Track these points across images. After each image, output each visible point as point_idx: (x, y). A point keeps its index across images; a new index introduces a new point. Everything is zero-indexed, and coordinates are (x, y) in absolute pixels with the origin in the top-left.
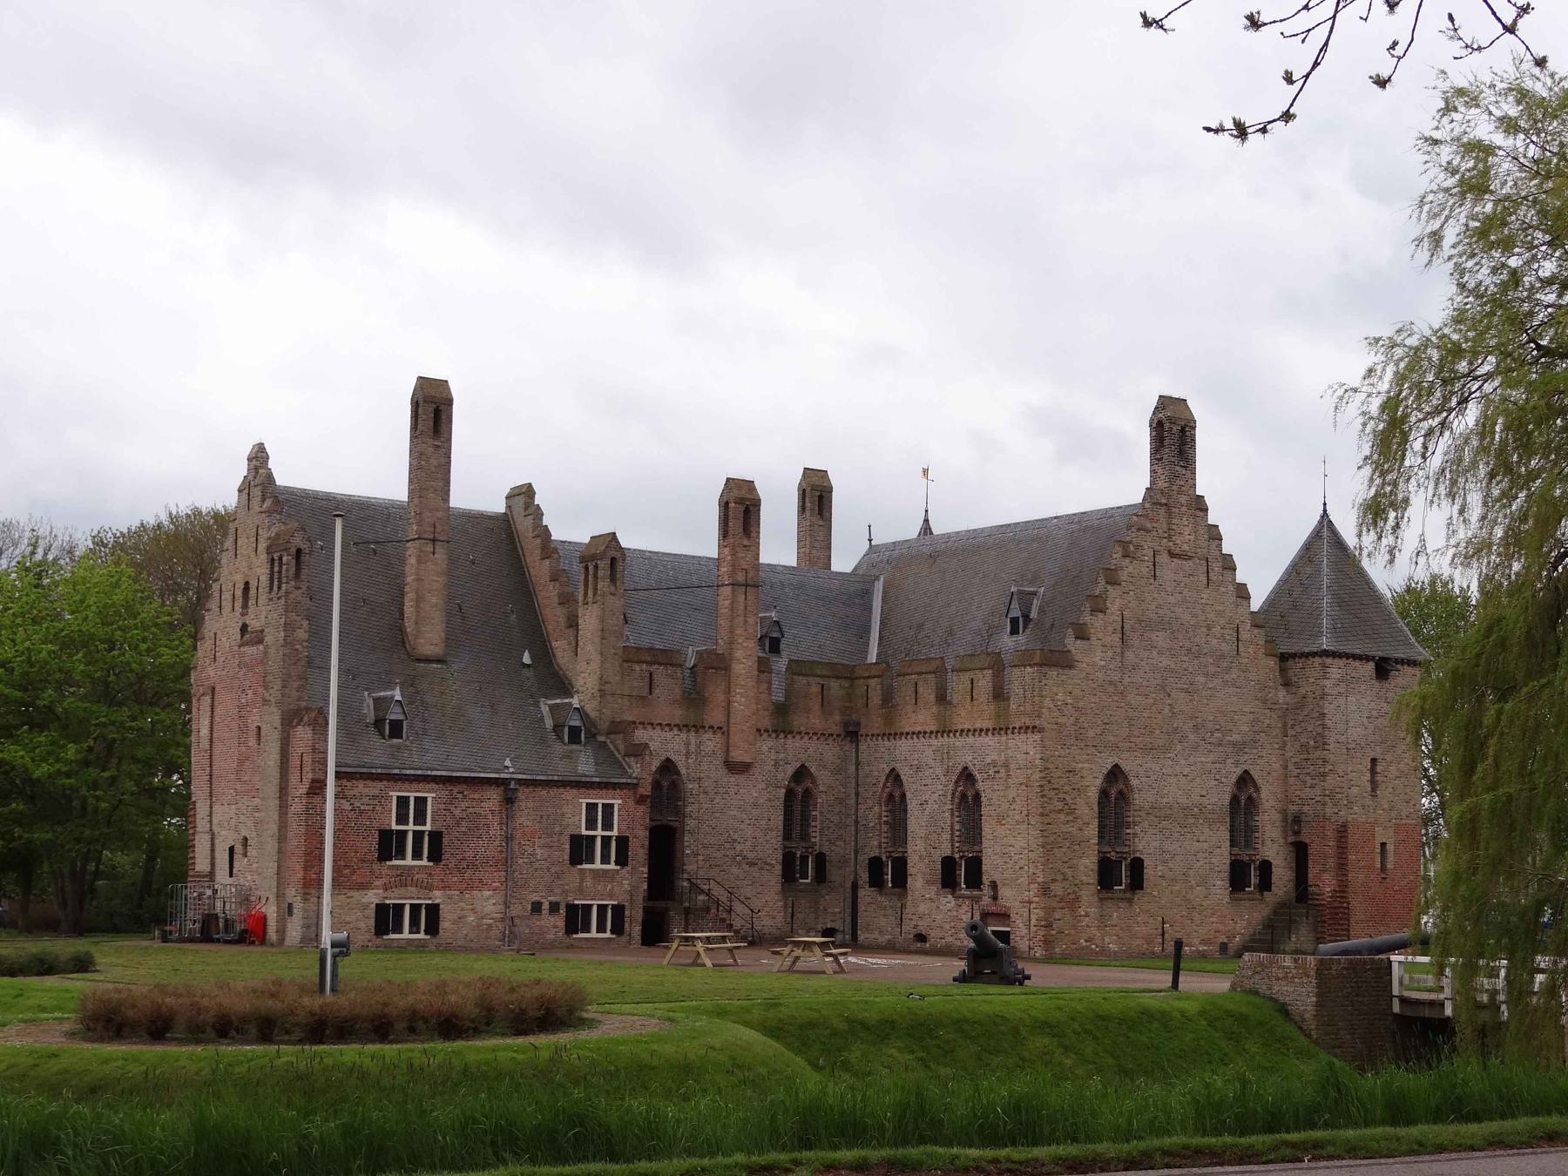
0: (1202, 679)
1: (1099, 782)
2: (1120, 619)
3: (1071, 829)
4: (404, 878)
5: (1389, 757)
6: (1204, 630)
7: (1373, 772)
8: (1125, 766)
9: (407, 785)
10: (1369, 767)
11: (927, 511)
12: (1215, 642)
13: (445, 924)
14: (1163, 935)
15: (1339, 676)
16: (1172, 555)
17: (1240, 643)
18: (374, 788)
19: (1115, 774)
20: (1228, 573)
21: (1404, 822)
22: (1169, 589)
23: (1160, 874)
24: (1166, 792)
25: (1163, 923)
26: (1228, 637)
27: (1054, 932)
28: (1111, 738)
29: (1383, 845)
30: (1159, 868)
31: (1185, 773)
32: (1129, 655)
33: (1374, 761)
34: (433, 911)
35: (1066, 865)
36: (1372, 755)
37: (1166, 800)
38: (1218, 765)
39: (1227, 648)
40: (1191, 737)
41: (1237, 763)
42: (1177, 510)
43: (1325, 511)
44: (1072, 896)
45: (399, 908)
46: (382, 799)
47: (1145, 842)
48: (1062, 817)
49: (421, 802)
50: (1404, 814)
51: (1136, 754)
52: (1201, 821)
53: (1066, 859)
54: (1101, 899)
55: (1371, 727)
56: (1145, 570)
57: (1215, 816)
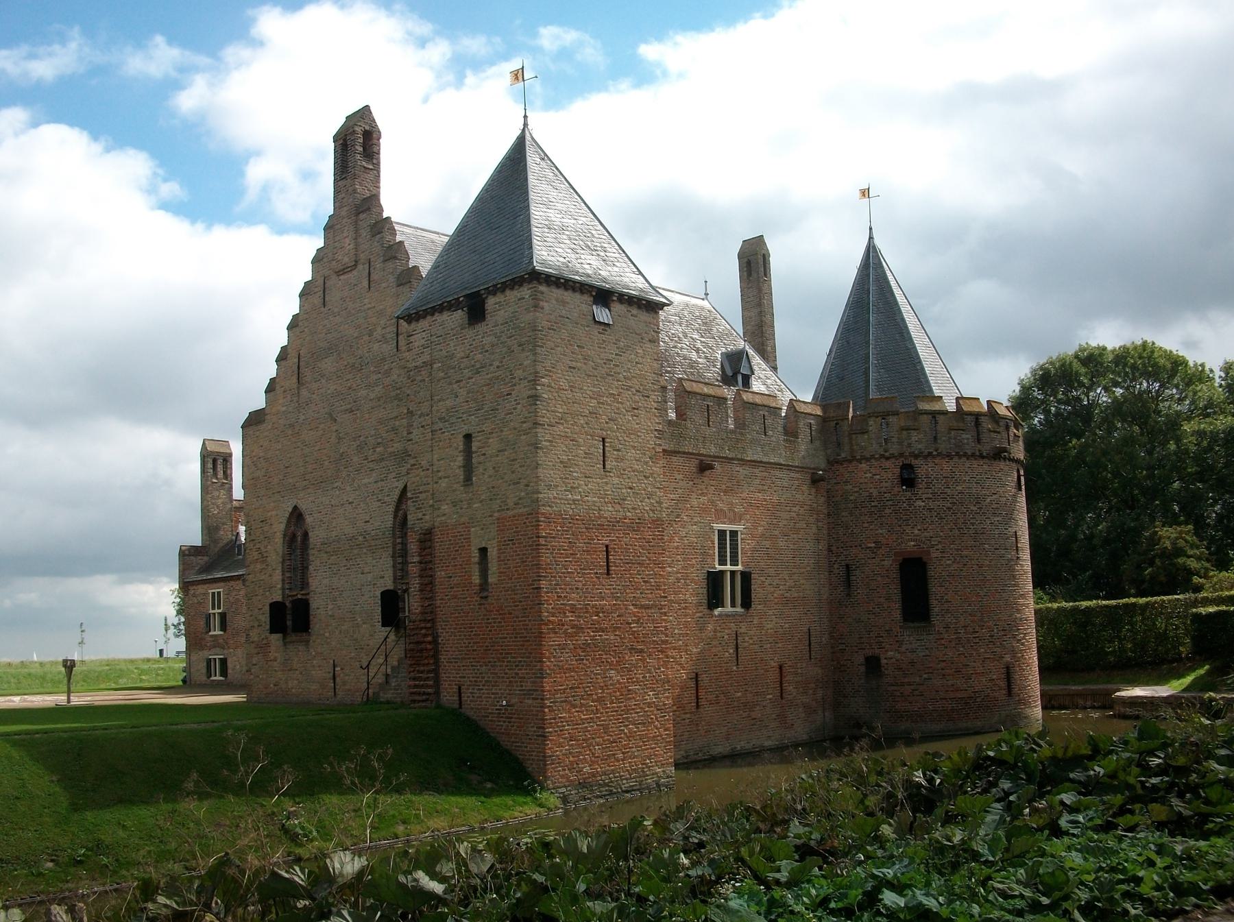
0: (363, 393)
1: (282, 526)
2: (296, 360)
3: (263, 577)
4: (216, 643)
5: (487, 427)
6: (366, 338)
7: (468, 452)
8: (303, 507)
9: (215, 585)
10: (461, 447)
11: (871, 229)
12: (376, 346)
13: (230, 671)
14: (334, 678)
15: (423, 342)
16: (339, 273)
17: (401, 337)
18: (206, 586)
19: (297, 516)
20: (390, 265)
21: (510, 513)
22: (336, 310)
23: (330, 613)
24: (334, 525)
25: (334, 666)
26: (389, 336)
27: (252, 677)
28: (291, 481)
29: (483, 551)
30: (330, 607)
31: (351, 500)
32: (304, 392)
33: (468, 437)
34: (224, 662)
35: (261, 612)
36: (465, 429)
37: (334, 533)
38: (380, 484)
39: (388, 348)
40: (355, 459)
41: (398, 478)
42: (339, 226)
43: (525, 125)
44: (264, 642)
45: (215, 659)
46: (206, 594)
47: (320, 581)
48: (259, 566)
49: (219, 593)
50: (511, 503)
51: (309, 490)
52: (365, 550)
53: (260, 607)
54: (285, 644)
55: (463, 392)
56: (317, 300)
57: (378, 542)
